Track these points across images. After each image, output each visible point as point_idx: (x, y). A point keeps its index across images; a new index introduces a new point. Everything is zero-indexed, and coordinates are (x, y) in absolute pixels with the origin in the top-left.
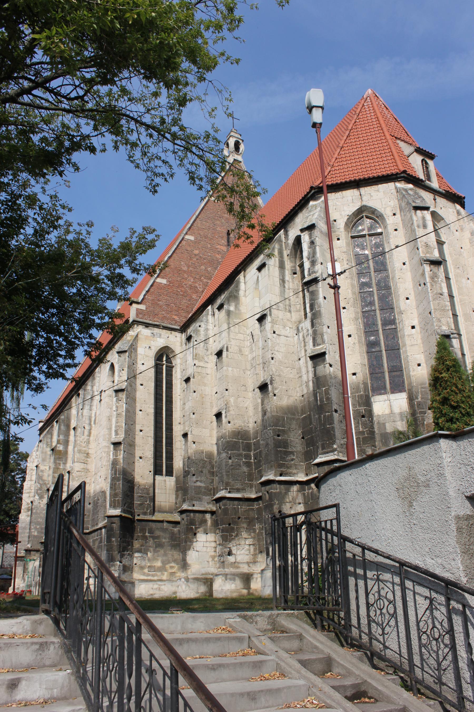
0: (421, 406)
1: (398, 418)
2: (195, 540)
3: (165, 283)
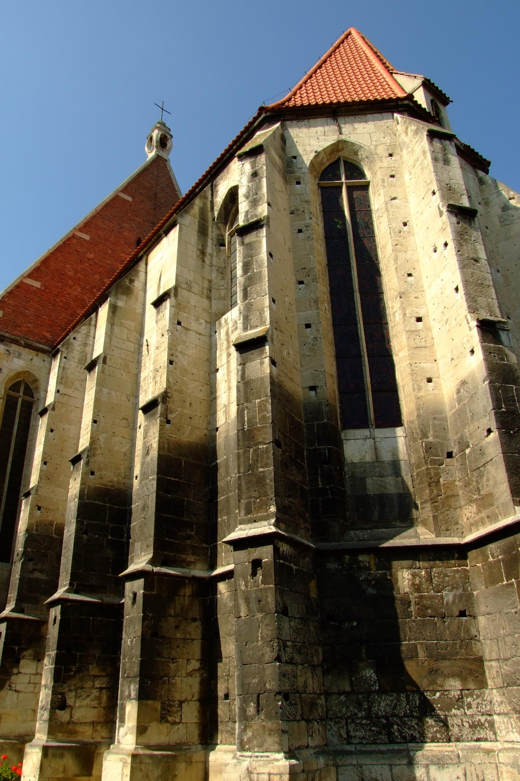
0: (433, 450)
2: (15, 671)
3: (39, 287)
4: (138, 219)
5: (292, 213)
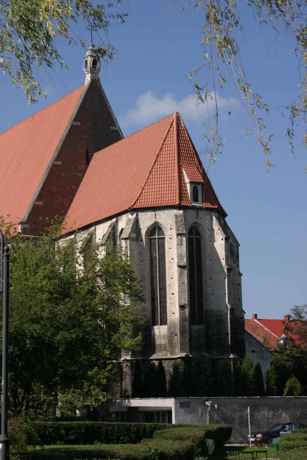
1: (162, 338)
4: (85, 136)
5: (139, 253)
